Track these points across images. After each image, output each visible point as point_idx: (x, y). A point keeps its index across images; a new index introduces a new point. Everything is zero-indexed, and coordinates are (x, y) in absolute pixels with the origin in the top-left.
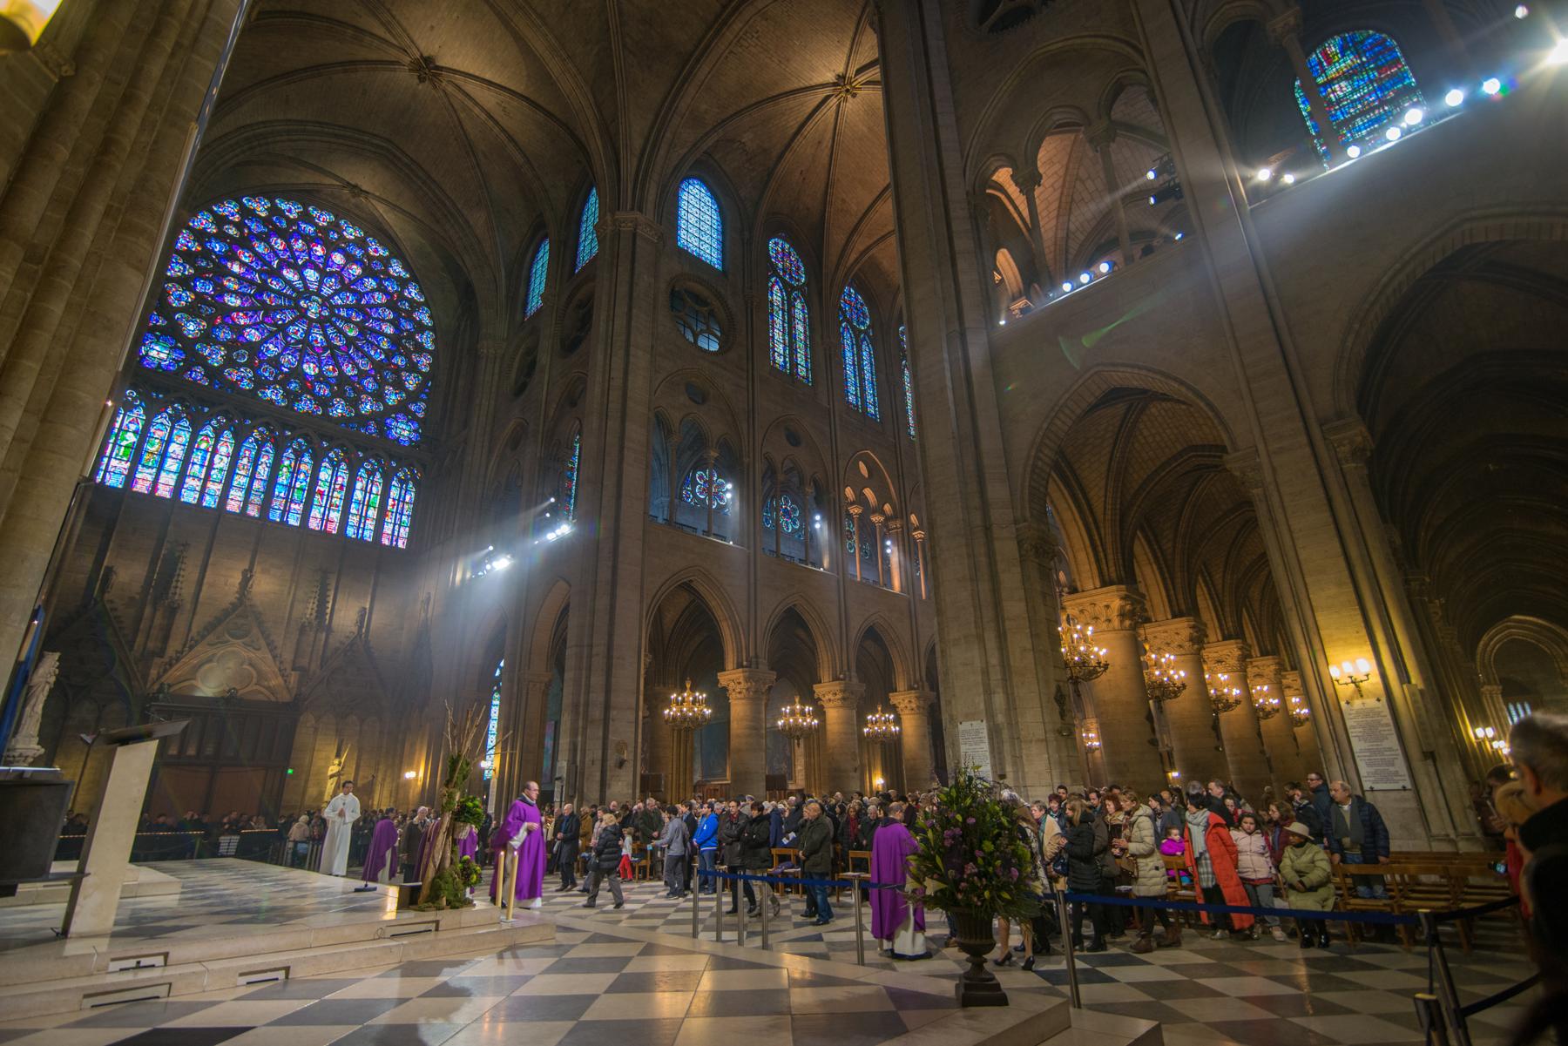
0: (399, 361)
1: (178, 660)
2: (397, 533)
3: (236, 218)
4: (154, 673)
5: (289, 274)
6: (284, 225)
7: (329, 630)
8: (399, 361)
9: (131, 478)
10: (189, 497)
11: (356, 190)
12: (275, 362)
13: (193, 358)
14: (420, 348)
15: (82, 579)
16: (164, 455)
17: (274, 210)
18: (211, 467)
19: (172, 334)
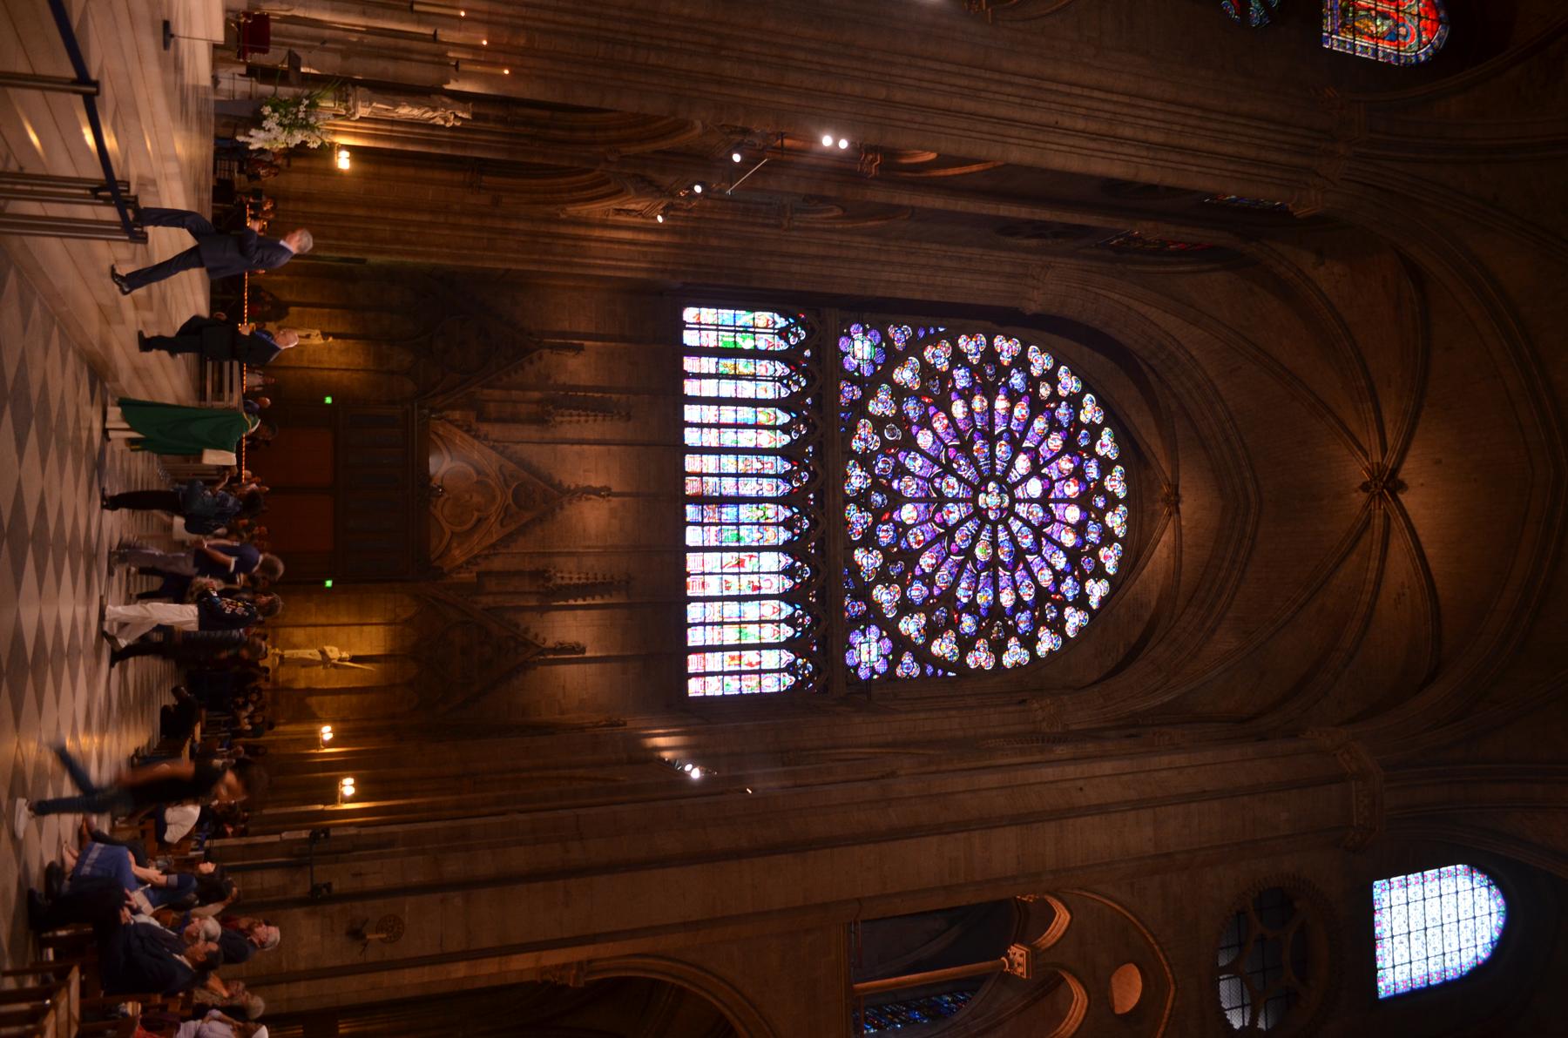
0: (968, 624)
1: (476, 437)
2: (708, 680)
3: (1062, 392)
4: (457, 415)
5: (1022, 464)
6: (1084, 443)
7: (544, 609)
8: (968, 624)
9: (700, 352)
10: (691, 413)
11: (1174, 501)
12: (901, 471)
13: (869, 386)
14: (998, 648)
15: (565, 325)
16: (737, 377)
17: (1095, 431)
18: (737, 426)
19: (891, 357)
